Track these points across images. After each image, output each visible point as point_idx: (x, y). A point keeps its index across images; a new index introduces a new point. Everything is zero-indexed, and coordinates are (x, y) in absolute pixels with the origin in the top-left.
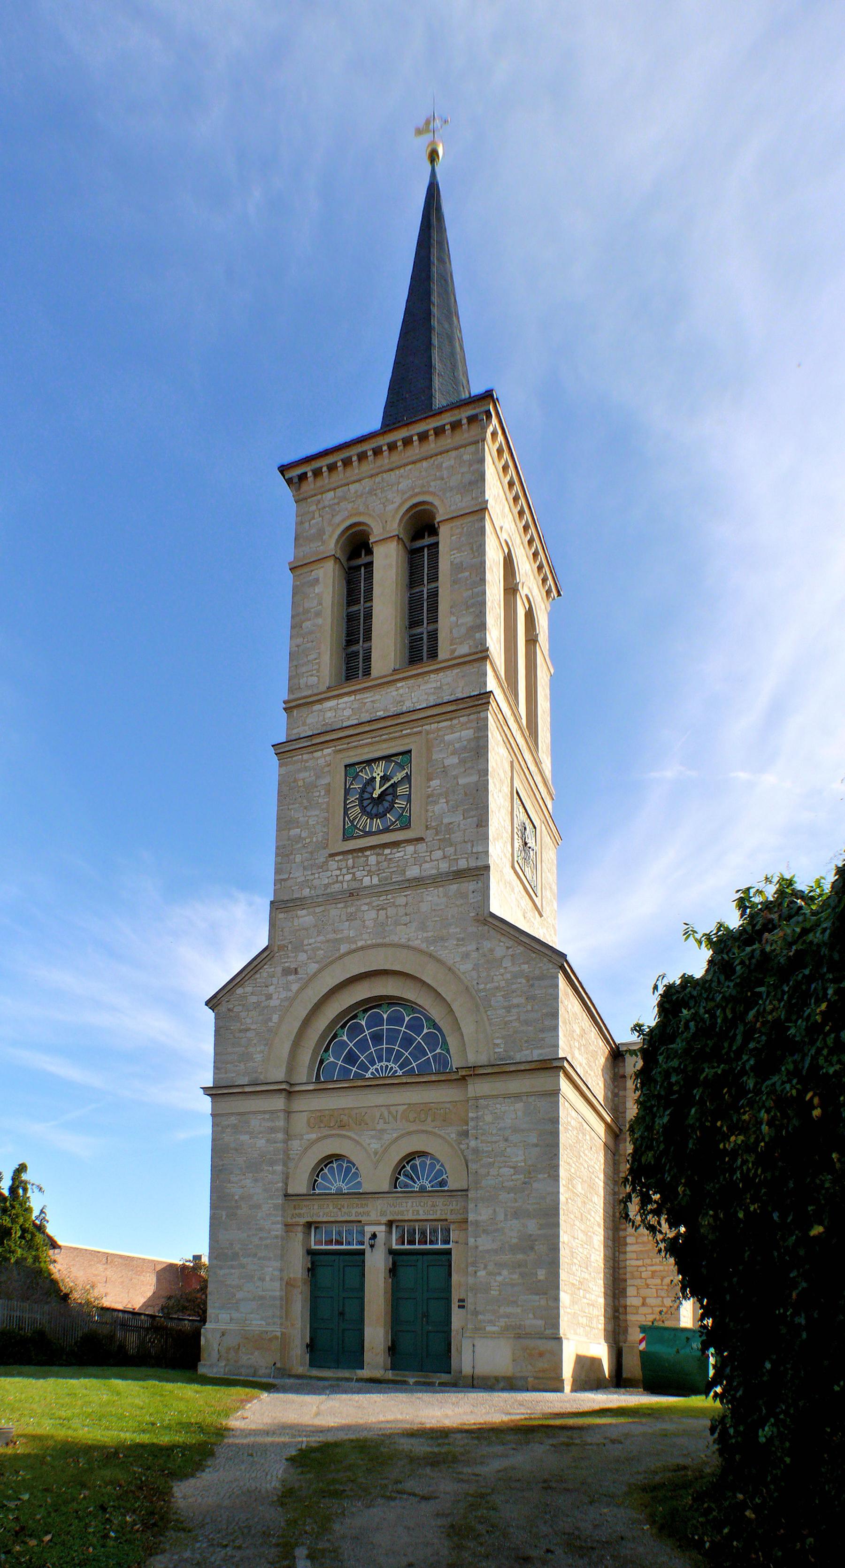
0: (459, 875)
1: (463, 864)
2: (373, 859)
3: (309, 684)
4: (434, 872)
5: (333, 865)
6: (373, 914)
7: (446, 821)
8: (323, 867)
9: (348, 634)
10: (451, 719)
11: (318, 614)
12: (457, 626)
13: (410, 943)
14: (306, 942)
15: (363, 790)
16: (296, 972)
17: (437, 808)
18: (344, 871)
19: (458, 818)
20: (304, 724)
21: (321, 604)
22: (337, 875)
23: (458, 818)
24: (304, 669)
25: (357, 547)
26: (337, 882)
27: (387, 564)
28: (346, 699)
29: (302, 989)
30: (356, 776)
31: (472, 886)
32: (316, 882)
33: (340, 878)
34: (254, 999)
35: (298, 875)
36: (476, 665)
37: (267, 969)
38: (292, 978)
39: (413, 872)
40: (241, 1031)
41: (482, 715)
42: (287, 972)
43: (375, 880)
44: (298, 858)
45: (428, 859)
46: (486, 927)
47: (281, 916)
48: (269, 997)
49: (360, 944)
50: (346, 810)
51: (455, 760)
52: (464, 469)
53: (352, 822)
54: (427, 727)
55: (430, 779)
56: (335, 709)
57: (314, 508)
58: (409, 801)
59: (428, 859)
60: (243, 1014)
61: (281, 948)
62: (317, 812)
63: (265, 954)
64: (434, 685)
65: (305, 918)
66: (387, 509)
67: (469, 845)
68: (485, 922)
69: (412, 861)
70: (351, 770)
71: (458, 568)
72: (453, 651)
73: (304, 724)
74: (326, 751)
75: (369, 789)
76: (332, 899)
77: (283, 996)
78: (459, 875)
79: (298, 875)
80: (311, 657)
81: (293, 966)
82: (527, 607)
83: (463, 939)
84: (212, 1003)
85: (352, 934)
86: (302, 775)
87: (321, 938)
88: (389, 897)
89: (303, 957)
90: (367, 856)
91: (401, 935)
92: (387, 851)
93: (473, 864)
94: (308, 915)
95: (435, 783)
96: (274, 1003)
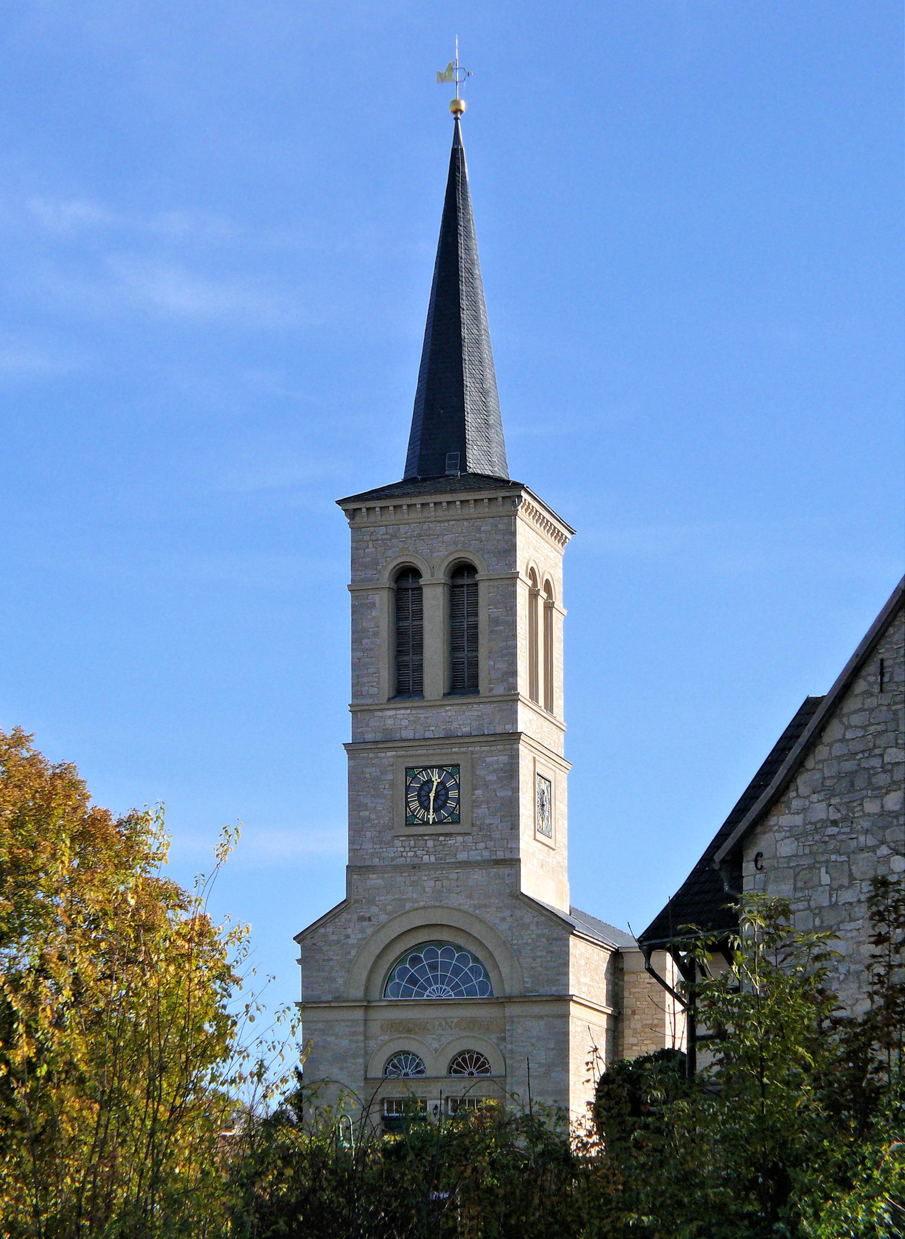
0: (498, 862)
1: (500, 855)
2: (430, 843)
3: (371, 693)
4: (479, 858)
5: (397, 843)
6: (432, 883)
7: (487, 822)
8: (390, 844)
9: (399, 645)
10: (491, 746)
11: (376, 634)
12: (494, 669)
13: (461, 907)
14: (377, 899)
15: (421, 789)
16: (370, 919)
17: (480, 811)
18: (408, 849)
19: (496, 821)
20: (367, 725)
21: (378, 627)
22: (400, 850)
23: (496, 821)
24: (365, 680)
25: (407, 576)
26: (402, 856)
27: (434, 604)
28: (402, 711)
29: (375, 933)
30: (414, 777)
31: (507, 871)
32: (384, 855)
33: (404, 854)
34: (335, 937)
35: (368, 847)
36: (510, 703)
37: (345, 916)
38: (365, 923)
39: (462, 856)
40: (324, 960)
41: (515, 746)
42: (362, 919)
43: (433, 859)
44: (368, 834)
45: (473, 848)
46: (518, 902)
47: (355, 877)
48: (348, 937)
49: (422, 904)
50: (407, 804)
51: (493, 777)
52: (500, 537)
53: (413, 812)
54: (472, 749)
55: (474, 789)
56: (394, 717)
57: (367, 538)
58: (458, 802)
59: (473, 848)
60: (325, 949)
61: (356, 901)
62: (383, 801)
63: (343, 906)
64: (476, 713)
65: (375, 880)
66: (435, 555)
67: (505, 842)
68: (517, 898)
69: (463, 847)
70: (411, 772)
71: (494, 621)
72: (491, 690)
73: (367, 725)
74: (389, 754)
75: (426, 788)
76: (397, 868)
77: (359, 936)
78: (498, 862)
79: (368, 847)
80: (370, 671)
81: (367, 915)
82: (574, 998)
83: (500, 908)
84: (298, 938)
85: (415, 896)
86: (367, 770)
87: (390, 897)
88: (444, 872)
89: (375, 909)
90: (426, 840)
91: (455, 900)
92: (441, 838)
93: (508, 856)
94: (378, 878)
95: (478, 792)
96: (351, 941)
